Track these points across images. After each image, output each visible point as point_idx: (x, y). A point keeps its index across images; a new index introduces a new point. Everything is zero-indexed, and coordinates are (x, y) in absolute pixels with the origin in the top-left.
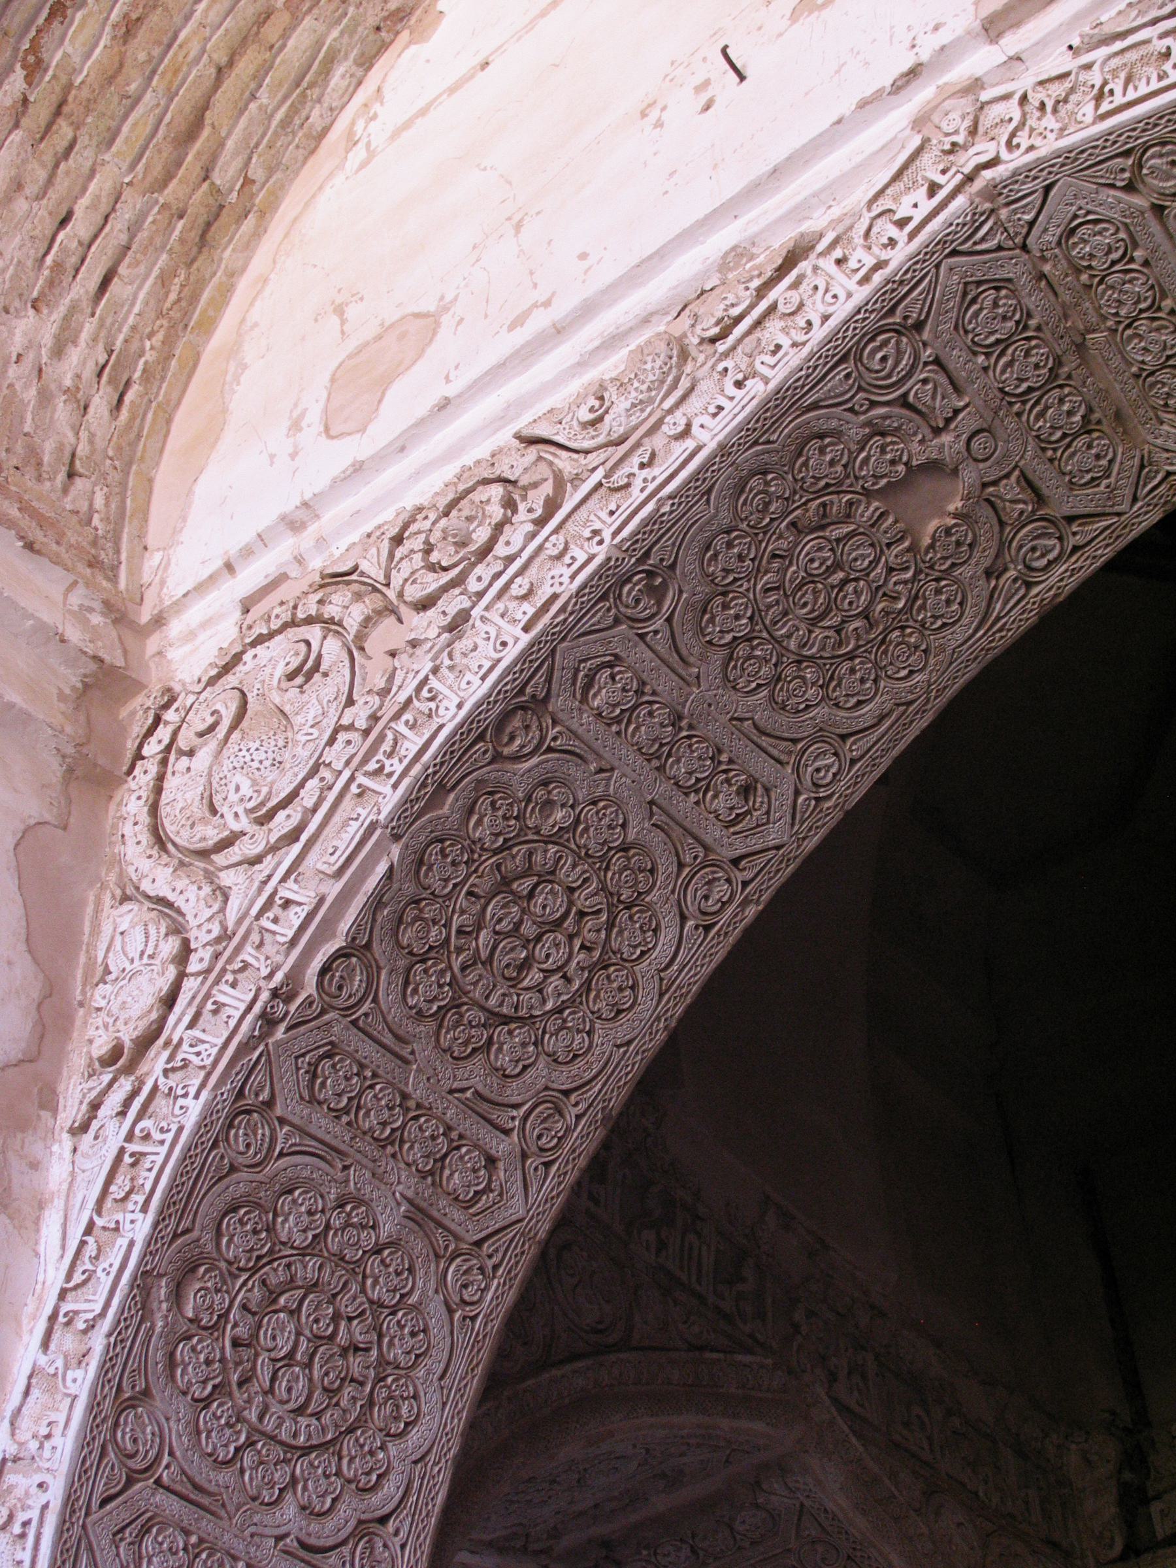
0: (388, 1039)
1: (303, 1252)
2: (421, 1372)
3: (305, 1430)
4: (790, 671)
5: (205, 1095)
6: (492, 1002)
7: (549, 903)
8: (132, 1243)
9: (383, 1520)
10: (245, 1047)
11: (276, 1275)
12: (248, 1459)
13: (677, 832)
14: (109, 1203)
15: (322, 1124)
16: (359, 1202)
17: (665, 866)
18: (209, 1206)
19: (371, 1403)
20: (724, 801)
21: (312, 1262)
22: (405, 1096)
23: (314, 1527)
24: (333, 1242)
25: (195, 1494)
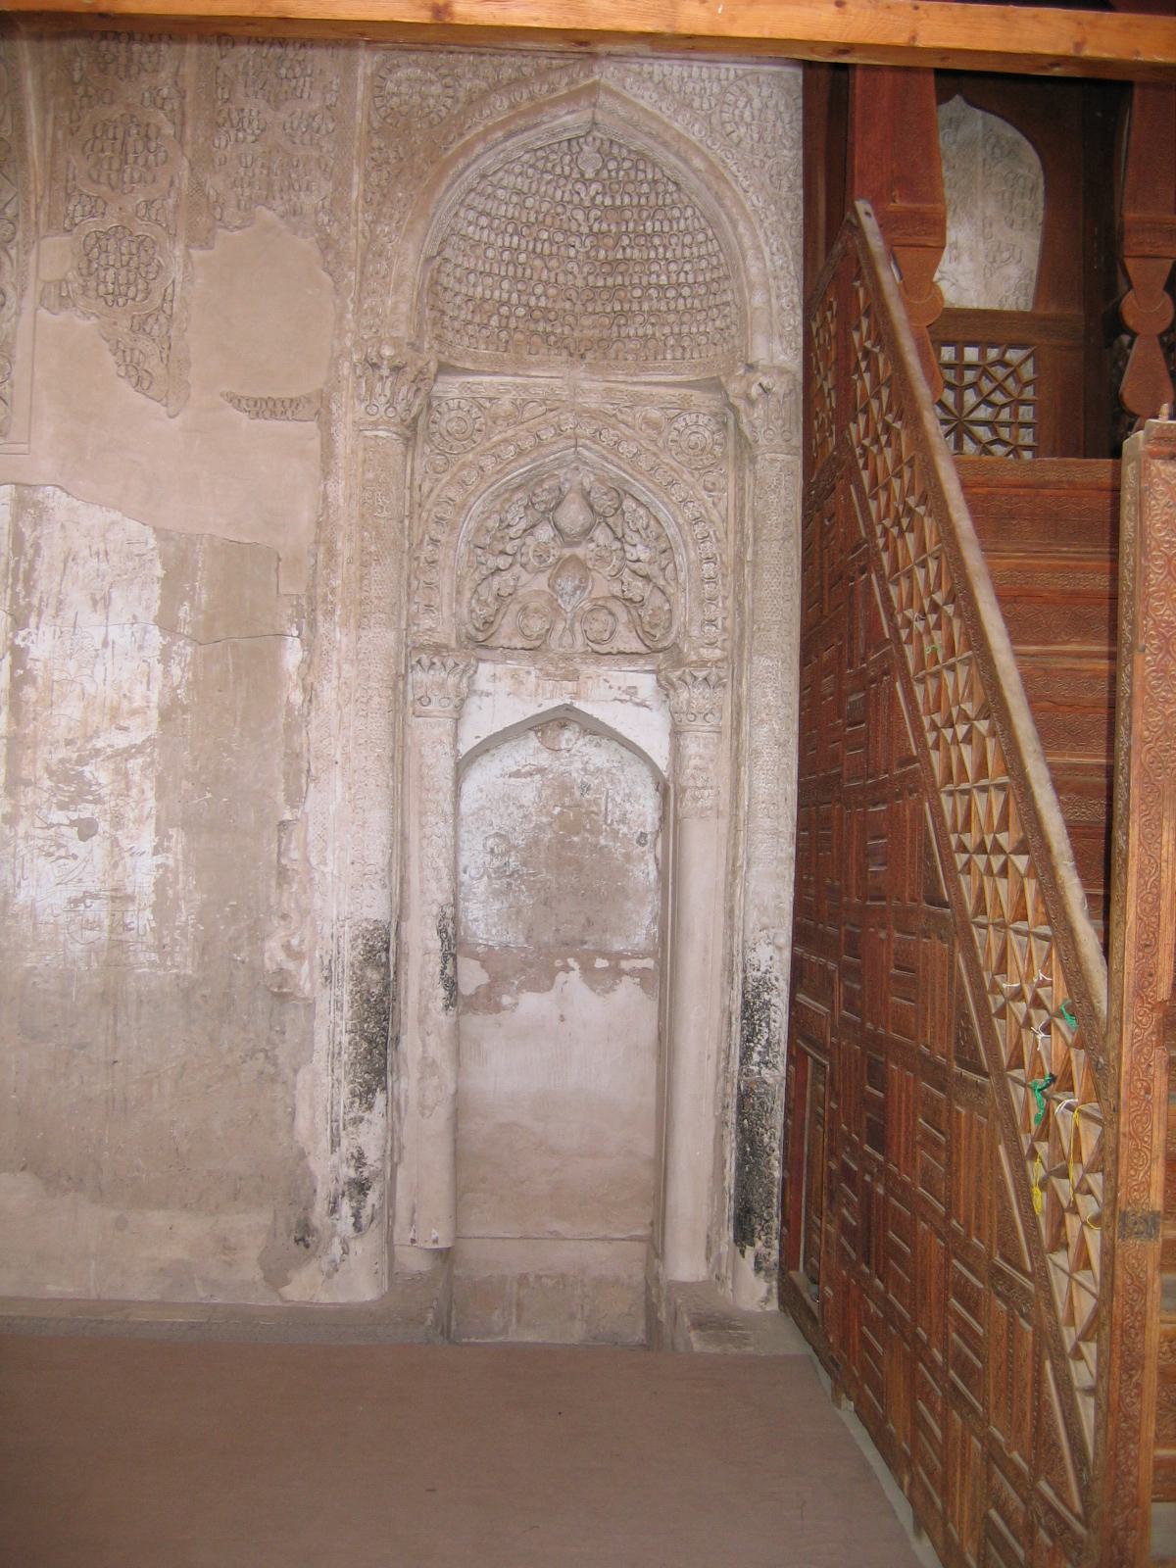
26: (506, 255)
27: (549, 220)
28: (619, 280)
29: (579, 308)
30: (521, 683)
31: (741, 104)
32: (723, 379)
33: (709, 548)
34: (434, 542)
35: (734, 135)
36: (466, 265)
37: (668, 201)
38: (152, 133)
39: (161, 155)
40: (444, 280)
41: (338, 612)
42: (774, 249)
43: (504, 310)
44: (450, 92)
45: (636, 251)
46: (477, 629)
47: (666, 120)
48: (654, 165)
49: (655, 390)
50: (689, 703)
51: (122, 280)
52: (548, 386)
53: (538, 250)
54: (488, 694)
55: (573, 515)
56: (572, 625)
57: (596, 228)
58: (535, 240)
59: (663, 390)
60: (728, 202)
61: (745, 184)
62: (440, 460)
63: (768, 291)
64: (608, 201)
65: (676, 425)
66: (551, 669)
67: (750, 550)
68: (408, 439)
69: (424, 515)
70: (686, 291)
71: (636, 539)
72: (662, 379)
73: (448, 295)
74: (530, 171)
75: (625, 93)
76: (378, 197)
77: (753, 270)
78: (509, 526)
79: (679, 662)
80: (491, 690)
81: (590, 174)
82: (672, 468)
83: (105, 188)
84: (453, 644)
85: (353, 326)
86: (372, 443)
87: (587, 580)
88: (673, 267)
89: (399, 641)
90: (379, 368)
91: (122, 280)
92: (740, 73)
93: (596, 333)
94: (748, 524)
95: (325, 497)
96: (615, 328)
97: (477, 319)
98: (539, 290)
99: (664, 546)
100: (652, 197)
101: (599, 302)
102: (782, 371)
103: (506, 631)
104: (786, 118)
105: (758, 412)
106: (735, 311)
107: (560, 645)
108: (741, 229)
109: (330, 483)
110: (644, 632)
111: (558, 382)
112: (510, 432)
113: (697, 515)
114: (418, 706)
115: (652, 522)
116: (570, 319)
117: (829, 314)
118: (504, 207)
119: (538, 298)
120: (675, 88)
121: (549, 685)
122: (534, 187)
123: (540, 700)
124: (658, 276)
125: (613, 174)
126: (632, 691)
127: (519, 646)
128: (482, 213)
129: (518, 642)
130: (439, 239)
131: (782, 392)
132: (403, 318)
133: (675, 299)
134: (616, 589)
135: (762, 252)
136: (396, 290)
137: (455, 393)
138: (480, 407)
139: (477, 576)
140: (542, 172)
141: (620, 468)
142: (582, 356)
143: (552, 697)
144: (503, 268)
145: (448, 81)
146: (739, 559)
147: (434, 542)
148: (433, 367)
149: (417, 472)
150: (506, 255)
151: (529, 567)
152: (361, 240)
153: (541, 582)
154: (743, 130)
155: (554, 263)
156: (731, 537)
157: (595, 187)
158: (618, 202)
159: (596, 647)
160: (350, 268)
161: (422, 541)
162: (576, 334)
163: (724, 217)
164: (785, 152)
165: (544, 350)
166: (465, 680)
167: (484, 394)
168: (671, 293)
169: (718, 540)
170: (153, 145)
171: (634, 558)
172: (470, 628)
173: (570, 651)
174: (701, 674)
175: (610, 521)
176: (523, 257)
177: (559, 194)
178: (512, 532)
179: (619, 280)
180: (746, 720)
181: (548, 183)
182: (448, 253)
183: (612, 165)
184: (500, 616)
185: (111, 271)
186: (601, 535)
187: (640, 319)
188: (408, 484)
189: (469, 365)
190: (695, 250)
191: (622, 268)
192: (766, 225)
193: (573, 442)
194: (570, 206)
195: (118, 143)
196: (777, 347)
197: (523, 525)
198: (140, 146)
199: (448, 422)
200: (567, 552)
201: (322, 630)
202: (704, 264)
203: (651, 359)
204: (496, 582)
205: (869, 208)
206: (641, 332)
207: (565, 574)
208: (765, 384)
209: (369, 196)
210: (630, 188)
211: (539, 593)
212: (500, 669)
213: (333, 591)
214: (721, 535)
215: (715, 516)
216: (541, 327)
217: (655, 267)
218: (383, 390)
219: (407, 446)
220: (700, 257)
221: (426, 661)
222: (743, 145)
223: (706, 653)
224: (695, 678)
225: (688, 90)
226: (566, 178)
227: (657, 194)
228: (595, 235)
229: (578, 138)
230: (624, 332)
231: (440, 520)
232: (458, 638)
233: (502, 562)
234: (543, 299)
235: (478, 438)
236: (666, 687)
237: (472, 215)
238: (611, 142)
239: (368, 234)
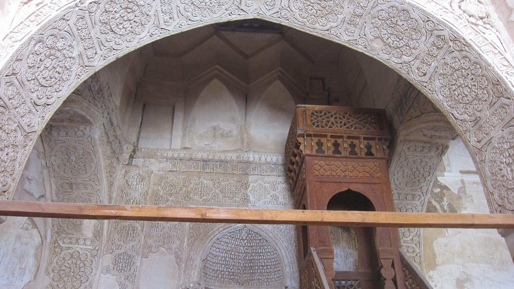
0: (93, 22)
1: (59, 50)
2: (66, 83)
3: (43, 82)
4: (190, 4)
5: (59, 12)
6: (112, 27)
7: (131, 16)
8: (31, 31)
9: (48, 105)
10: (70, 8)
11: (53, 52)
12: (33, 82)
13: (157, 18)
14: (27, 20)
15: (74, 30)
16: (72, 47)
17: (152, 22)
18: (49, 32)
19: (56, 84)
20: (167, 18)
21: (60, 53)
22: (90, 33)
23: (37, 100)
24: (65, 52)
25: (22, 83)
27: (234, 250)
28: (252, 264)
29: (242, 272)
38: (135, 229)
39: (137, 234)
40: (207, 265)
43: (223, 273)
51: (124, 266)
60: (279, 245)
64: (249, 245)
70: (269, 267)
73: (208, 270)
77: (286, 262)
81: (244, 238)
83: (122, 242)
85: (183, 278)
88: (266, 261)
91: (124, 266)
93: (246, 278)
98: (232, 267)
108: (282, 251)
136: (195, 269)
150: (223, 259)
152: (186, 256)
155: (235, 260)
165: (233, 283)
168: (265, 268)
170: (135, 232)
182: (208, 258)
183: (250, 236)
185: (121, 264)
187: (257, 275)
191: (253, 261)
195: (127, 232)
196: (293, 282)
198: (132, 232)
202: (273, 260)
205: (314, 249)
206: (258, 278)
210: (254, 241)
217: (261, 261)
237: (215, 249)
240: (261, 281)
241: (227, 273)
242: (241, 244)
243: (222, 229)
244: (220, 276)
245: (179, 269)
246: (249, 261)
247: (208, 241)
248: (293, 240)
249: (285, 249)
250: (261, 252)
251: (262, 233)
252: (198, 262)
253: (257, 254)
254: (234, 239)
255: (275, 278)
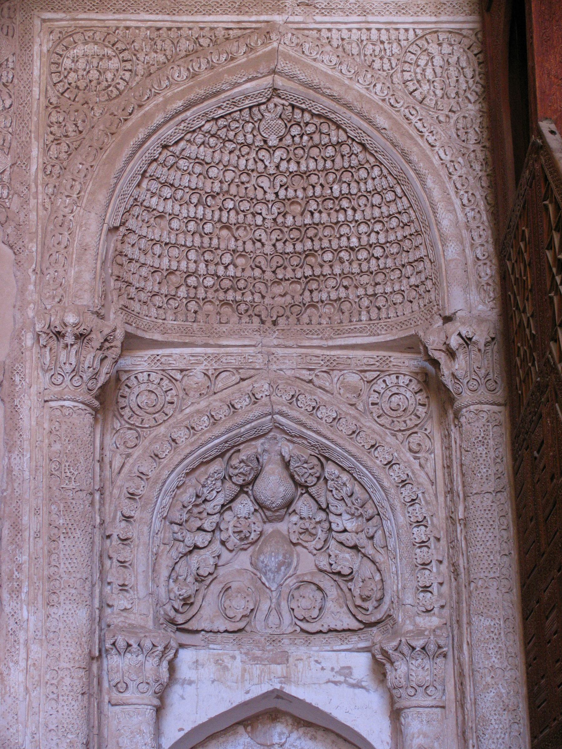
26: (192, 226)
28: (309, 245)
29: (269, 275)
30: (226, 668)
31: (422, 63)
32: (421, 334)
33: (419, 511)
34: (127, 518)
35: (416, 94)
36: (150, 236)
37: (354, 162)
41: (25, 590)
42: (465, 201)
43: (192, 281)
44: (128, 66)
45: (324, 215)
46: (176, 611)
47: (347, 82)
48: (339, 127)
49: (351, 353)
50: (408, 677)
52: (240, 355)
53: (224, 220)
54: (190, 683)
55: (273, 485)
56: (279, 604)
57: (282, 194)
58: (221, 210)
59: (359, 353)
60: (414, 158)
61: (431, 139)
62: (130, 434)
63: (462, 243)
64: (293, 167)
65: (376, 387)
66: (258, 653)
67: (461, 508)
68: (96, 410)
69: (116, 492)
70: (378, 252)
71: (341, 508)
72: (359, 341)
73: (133, 266)
74: (212, 141)
75: (304, 58)
76: (57, 169)
77: (445, 223)
78: (205, 501)
79: (395, 634)
80: (194, 677)
81: (273, 141)
82: (374, 431)
84: (150, 624)
85: (35, 297)
86: (58, 413)
87: (291, 555)
88: (363, 228)
89: (91, 619)
90: (64, 336)
92: (419, 32)
94: (458, 480)
95: (10, 471)
96: (307, 293)
97: (164, 291)
98: (227, 259)
99: (371, 511)
100: (338, 159)
101: (289, 269)
102: (480, 320)
103: (207, 615)
104: (469, 72)
105: (460, 365)
106: (428, 265)
107: (267, 626)
108: (430, 183)
109: (14, 456)
110: (357, 606)
111: (251, 350)
112: (203, 404)
113: (404, 477)
114: (115, 696)
115: (357, 488)
116: (262, 287)
117: (522, 245)
118: (187, 177)
119: (226, 268)
120: (355, 51)
121: (256, 670)
122: (217, 156)
123: (247, 686)
124: (348, 239)
125: (297, 139)
126: (347, 671)
127: (222, 629)
128: (164, 184)
129: (221, 624)
130: (122, 210)
131: (482, 342)
132: (86, 287)
133: (368, 260)
134: (324, 563)
135: (452, 204)
137: (144, 366)
138: (172, 379)
139: (174, 554)
140: (224, 141)
141: (319, 434)
142: (275, 323)
143: (260, 683)
144: (189, 239)
145: (126, 55)
146: (451, 519)
147: (127, 518)
148: (120, 335)
149: (107, 448)
150: (192, 226)
151: (230, 545)
152: (41, 213)
153: (243, 560)
154: (426, 87)
155: (241, 232)
156: (441, 499)
157: (278, 153)
158: (303, 168)
159: (304, 626)
160: (31, 240)
161: (114, 518)
162: (267, 300)
163: (412, 173)
164: (470, 106)
165: (235, 319)
166: (165, 664)
167: (173, 366)
168: (363, 255)
169: (427, 503)
171: (340, 528)
172: (168, 607)
173: (278, 631)
174: (418, 643)
175: (312, 490)
176: (208, 228)
177: (242, 162)
178: (209, 507)
179: (309, 245)
180: (469, 688)
181: (231, 152)
182: (132, 223)
183: (295, 131)
184: (200, 597)
186: (304, 505)
188: (97, 457)
189: (157, 337)
190: (384, 209)
191: (311, 233)
192: (454, 177)
193: (268, 409)
194: (255, 174)
196: (474, 297)
197: (220, 500)
199: (136, 396)
200: (269, 528)
201: (7, 609)
202: (394, 222)
203: (346, 322)
204: (194, 559)
206: (334, 296)
207: (267, 549)
208: (464, 334)
209: (49, 168)
210: (315, 152)
211: (241, 572)
212: (203, 654)
213: (19, 568)
214: (430, 497)
215: (423, 478)
216: (230, 296)
217: (344, 230)
218: (68, 358)
219: (96, 419)
220: (390, 216)
221: (121, 644)
222: (427, 101)
223: (424, 622)
224: (414, 648)
225: (368, 53)
226: (249, 145)
227: (343, 156)
228: (282, 201)
229: (259, 105)
230: (316, 296)
231: (132, 496)
232: (156, 619)
233: (201, 539)
234: (231, 267)
235: (169, 410)
236: (380, 667)
237: (154, 186)
238: (293, 107)
239: (48, 206)
240: (346, 306)
241: (209, 282)
242: (260, 166)
243: (179, 104)
244: (182, 292)
245: (18, 263)
246: (295, 234)
247: (127, 151)
248: (472, 137)
249: (443, 173)
250: (342, 196)
251: (344, 116)
252: (89, 228)
253: (330, 204)
254: (230, 146)
255: (401, 292)
